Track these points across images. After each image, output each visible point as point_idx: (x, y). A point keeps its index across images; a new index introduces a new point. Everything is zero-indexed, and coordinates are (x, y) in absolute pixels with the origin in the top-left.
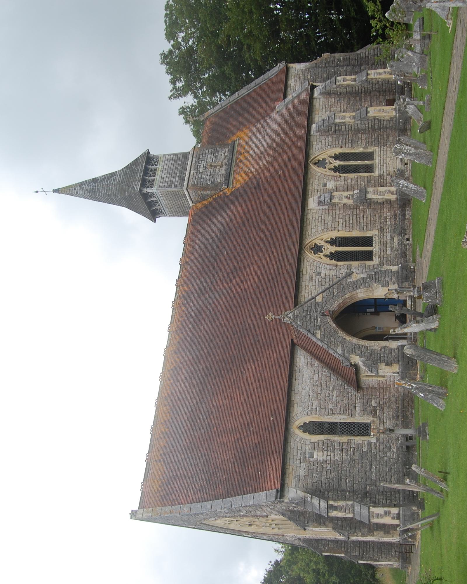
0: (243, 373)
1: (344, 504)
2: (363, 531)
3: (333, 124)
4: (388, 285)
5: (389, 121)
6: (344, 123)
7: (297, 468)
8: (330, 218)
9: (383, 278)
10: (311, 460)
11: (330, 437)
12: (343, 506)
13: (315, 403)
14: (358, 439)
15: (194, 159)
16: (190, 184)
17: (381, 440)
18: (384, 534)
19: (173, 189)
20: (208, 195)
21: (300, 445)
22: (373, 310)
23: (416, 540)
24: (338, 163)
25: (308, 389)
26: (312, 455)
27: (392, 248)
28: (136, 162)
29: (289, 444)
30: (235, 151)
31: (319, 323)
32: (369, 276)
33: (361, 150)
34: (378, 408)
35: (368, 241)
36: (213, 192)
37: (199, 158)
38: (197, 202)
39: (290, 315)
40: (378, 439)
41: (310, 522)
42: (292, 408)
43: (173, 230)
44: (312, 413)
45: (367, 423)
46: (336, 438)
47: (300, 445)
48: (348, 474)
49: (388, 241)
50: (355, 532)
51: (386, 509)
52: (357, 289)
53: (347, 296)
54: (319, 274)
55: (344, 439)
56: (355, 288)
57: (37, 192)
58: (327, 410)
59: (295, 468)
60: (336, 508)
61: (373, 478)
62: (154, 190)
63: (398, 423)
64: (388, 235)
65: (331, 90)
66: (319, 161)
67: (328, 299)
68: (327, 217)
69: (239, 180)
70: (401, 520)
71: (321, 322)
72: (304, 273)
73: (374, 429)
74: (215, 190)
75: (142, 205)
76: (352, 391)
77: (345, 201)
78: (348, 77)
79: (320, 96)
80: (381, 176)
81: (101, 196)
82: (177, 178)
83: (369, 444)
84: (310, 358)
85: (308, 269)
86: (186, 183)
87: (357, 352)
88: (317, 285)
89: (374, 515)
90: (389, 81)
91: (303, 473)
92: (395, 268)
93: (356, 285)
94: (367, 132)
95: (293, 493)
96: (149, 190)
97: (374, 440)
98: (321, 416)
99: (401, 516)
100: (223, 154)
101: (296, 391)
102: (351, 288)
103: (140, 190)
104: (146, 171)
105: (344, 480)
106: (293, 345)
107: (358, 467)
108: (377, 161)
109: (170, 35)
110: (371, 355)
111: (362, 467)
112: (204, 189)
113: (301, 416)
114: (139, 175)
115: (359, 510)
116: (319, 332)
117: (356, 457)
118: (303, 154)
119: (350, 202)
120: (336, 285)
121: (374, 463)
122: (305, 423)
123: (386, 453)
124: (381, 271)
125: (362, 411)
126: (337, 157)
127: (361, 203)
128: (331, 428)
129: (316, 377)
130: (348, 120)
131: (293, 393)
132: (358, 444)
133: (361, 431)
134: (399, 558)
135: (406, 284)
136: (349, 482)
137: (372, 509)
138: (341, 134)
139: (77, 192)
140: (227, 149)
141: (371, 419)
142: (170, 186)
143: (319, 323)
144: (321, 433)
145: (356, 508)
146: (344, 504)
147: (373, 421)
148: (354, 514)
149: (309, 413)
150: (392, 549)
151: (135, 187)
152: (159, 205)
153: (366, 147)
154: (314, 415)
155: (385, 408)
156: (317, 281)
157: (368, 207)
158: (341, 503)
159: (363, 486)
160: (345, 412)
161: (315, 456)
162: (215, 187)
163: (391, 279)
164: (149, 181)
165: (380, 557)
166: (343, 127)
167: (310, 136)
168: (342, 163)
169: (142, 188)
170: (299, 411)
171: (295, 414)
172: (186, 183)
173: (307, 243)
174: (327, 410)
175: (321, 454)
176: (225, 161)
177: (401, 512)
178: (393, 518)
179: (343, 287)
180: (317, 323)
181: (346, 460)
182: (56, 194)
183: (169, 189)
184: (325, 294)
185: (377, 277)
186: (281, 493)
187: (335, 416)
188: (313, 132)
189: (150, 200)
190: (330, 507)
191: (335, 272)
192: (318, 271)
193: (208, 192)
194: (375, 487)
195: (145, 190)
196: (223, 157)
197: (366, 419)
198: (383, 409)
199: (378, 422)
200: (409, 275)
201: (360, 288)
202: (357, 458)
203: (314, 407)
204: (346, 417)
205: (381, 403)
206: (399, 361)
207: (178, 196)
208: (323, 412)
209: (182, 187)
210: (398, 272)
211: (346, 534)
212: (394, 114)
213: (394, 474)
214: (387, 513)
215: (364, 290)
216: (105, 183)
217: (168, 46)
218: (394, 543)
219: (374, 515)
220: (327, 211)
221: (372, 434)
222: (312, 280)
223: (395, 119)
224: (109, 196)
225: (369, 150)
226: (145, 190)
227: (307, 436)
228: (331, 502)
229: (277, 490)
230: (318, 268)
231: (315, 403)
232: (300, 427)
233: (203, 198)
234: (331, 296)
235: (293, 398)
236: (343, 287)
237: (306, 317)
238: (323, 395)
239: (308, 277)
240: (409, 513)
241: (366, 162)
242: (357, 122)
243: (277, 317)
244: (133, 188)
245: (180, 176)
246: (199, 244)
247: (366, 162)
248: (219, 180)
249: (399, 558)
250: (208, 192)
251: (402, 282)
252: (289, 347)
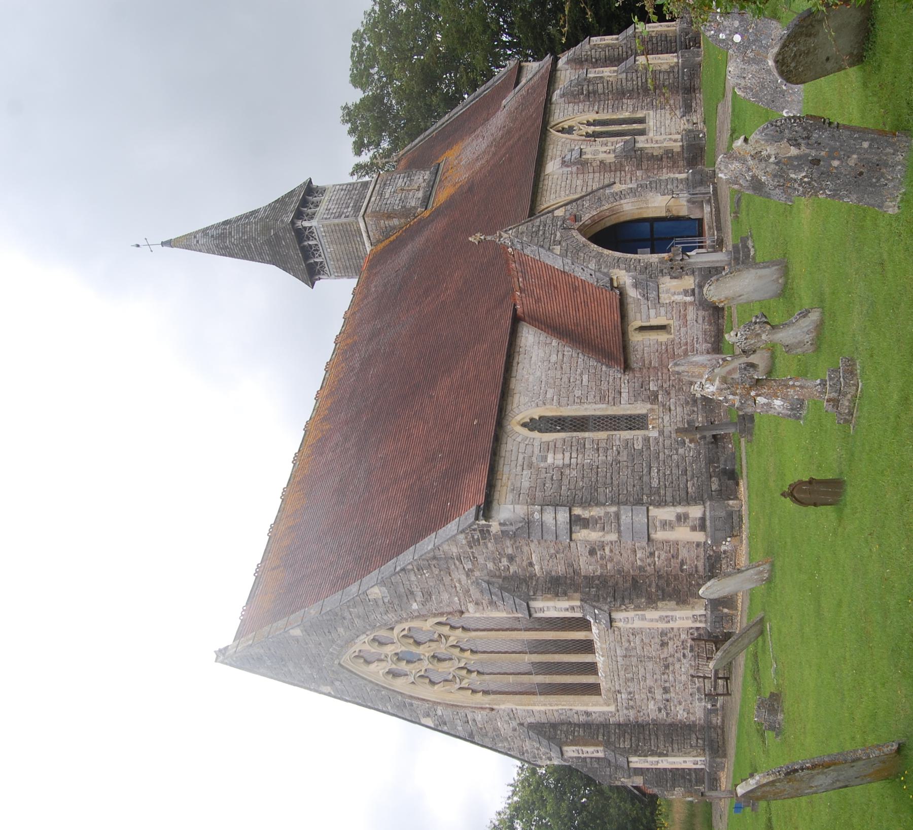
0: (431, 397)
1: (602, 514)
2: (637, 601)
3: (585, 79)
5: (669, 73)
6: (601, 77)
7: (515, 475)
8: (579, 182)
10: (542, 465)
11: (575, 434)
12: (600, 518)
14: (626, 434)
15: (378, 186)
16: (369, 210)
17: (666, 433)
18: (677, 604)
19: (343, 220)
20: (393, 228)
21: (522, 446)
23: (736, 609)
24: (591, 129)
25: (538, 374)
26: (545, 459)
28: (291, 194)
29: (503, 446)
30: (440, 172)
33: (626, 115)
34: (660, 392)
36: (402, 221)
37: (385, 184)
38: (379, 241)
40: (661, 432)
41: (539, 593)
42: (510, 398)
43: (337, 293)
45: (642, 415)
46: (586, 434)
47: (522, 446)
48: (609, 481)
50: (623, 603)
51: (680, 510)
52: (621, 199)
55: (602, 435)
57: (138, 246)
58: (571, 399)
59: (512, 477)
60: (585, 523)
61: (655, 484)
62: (314, 223)
63: (696, 409)
65: (584, 53)
66: (563, 129)
68: (574, 182)
69: (442, 196)
70: (708, 529)
71: (561, 236)
74: (407, 217)
75: (295, 253)
76: (614, 373)
77: (602, 156)
79: (566, 66)
81: (233, 244)
82: (350, 209)
83: (647, 440)
84: (543, 337)
86: (364, 235)
89: (658, 524)
90: (666, 37)
91: (526, 484)
94: (636, 95)
95: (507, 510)
96: (306, 224)
97: (653, 434)
99: (708, 523)
100: (421, 178)
103: (293, 223)
104: (304, 203)
105: (601, 490)
106: (516, 320)
107: (625, 472)
108: (651, 124)
109: (359, 79)
111: (633, 471)
112: (389, 216)
113: (524, 407)
114: (293, 206)
115: (629, 520)
117: (624, 457)
118: (540, 120)
119: (610, 158)
121: (654, 465)
122: (532, 419)
123: (677, 450)
125: (633, 398)
126: (589, 124)
127: (626, 157)
128: (579, 424)
129: (554, 358)
131: (513, 380)
132: (627, 440)
134: (704, 750)
136: (610, 492)
137: (654, 511)
138: (598, 99)
139: (198, 242)
140: (428, 172)
141: (649, 406)
142: (340, 216)
144: (563, 430)
145: (623, 517)
146: (602, 514)
147: (652, 410)
148: (619, 532)
150: (690, 734)
151: (283, 236)
152: (320, 256)
153: (633, 111)
154: (548, 406)
155: (673, 393)
157: (638, 165)
158: (596, 512)
159: (636, 496)
160: (602, 399)
161: (550, 460)
162: (406, 212)
164: (308, 215)
165: (670, 749)
166: (600, 86)
167: (551, 104)
169: (295, 220)
171: (515, 405)
172: (364, 235)
173: (543, 207)
174: (571, 399)
175: (559, 456)
176: (423, 185)
177: (708, 514)
178: (694, 529)
181: (605, 463)
182: (166, 249)
183: (337, 221)
184: (569, 207)
186: (486, 509)
187: (586, 406)
188: (554, 99)
189: (306, 243)
190: (575, 522)
193: (396, 222)
194: (657, 498)
195: (299, 224)
196: (421, 180)
197: (640, 408)
198: (669, 394)
202: (625, 459)
203: (549, 395)
204: (604, 406)
205: (665, 386)
207: (348, 234)
208: (564, 401)
209: (356, 217)
211: (606, 608)
212: (675, 60)
213: (692, 478)
214: (682, 519)
216: (242, 222)
217: (356, 96)
218: (695, 725)
219: (658, 524)
220: (574, 176)
221: (650, 427)
223: (676, 70)
224: (245, 241)
225: (640, 115)
226: (299, 224)
227: (536, 434)
228: (577, 511)
229: (478, 507)
232: (524, 425)
233: (386, 233)
235: (512, 386)
237: (537, 232)
238: (565, 379)
240: (723, 514)
242: (620, 77)
243: (489, 238)
244: (282, 221)
245: (354, 206)
246: (375, 286)
248: (413, 204)
249: (704, 750)
250: (396, 222)
252: (509, 322)
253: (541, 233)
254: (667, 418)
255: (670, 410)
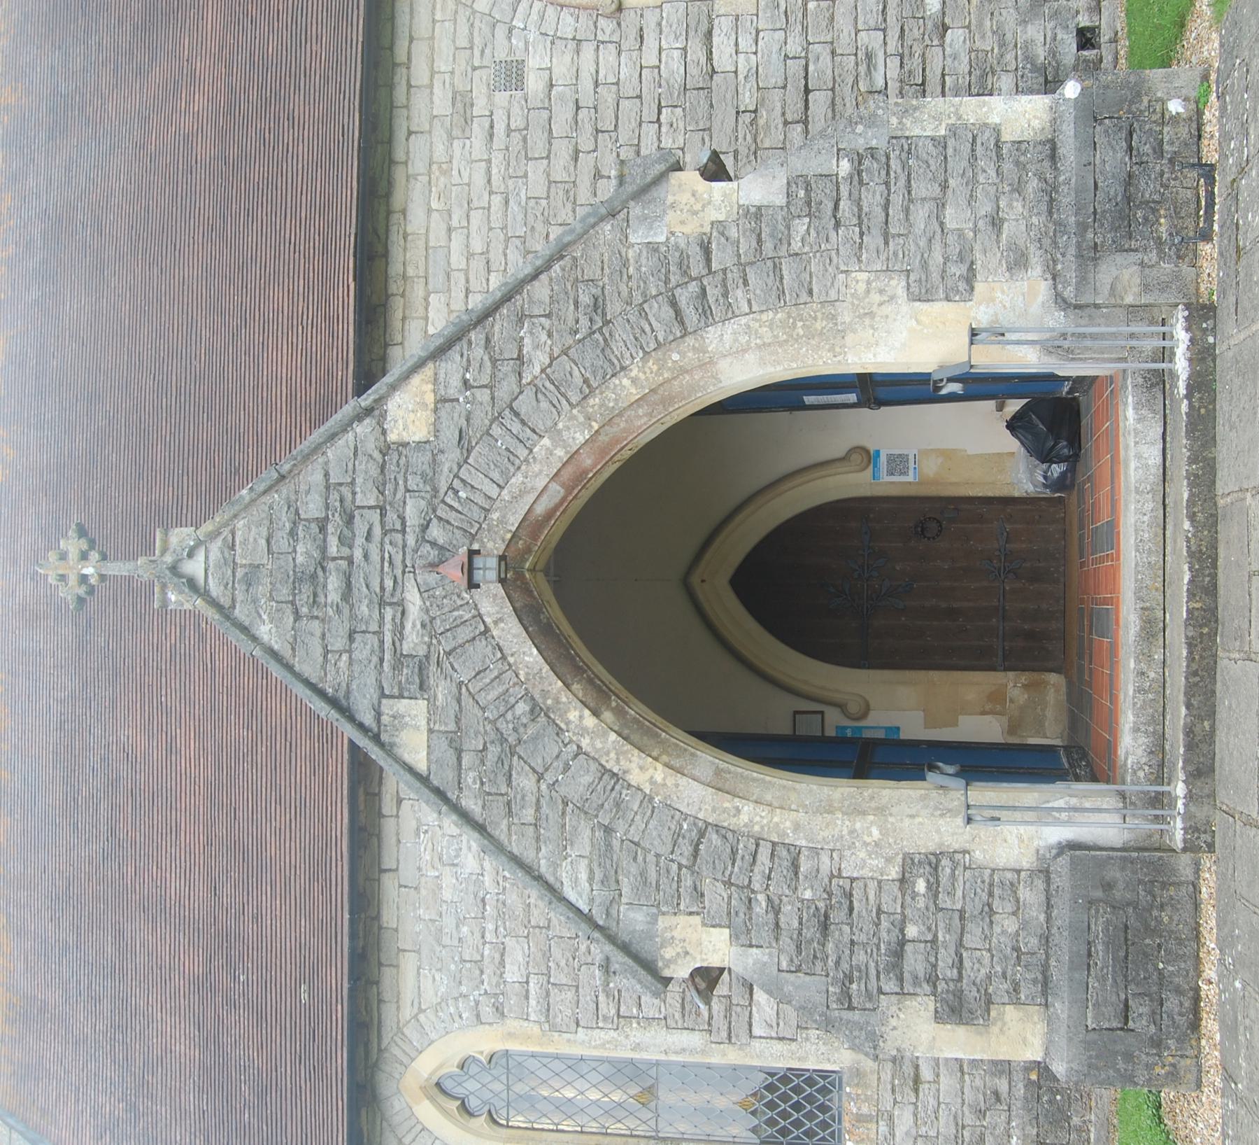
4: (970, 278)
9: (920, 214)
13: (516, 953)
22: (852, 398)
31: (413, 640)
32: (807, 196)
39: (195, 567)
42: (387, 972)
44: (499, 1011)
45: (824, 1074)
53: (626, 388)
54: (513, 75)
56: (691, 316)
67: (481, 419)
72: (420, 73)
73: (860, 1119)
85: (444, 46)
87: (715, 894)
88: (497, 158)
92: (1020, 114)
93: (696, 286)
98: (553, 1028)
101: (407, 873)
102: (660, 312)
110: (825, 926)
116: (415, 710)
120: (541, 290)
124: (908, 147)
131: (389, 884)
133: (784, 1115)
135: (1122, 275)
143: (413, 640)
147: (858, 1073)
149: (487, 1010)
154: (513, 1024)
156: (500, 128)
163: (996, 223)
170: (429, 997)
171: (407, 1012)
179: (597, 305)
180: (399, 631)
184: (451, 368)
185: (872, 198)
187: (636, 1034)
191: (608, 56)
192: (501, 55)
199: (887, 1076)
200: (1147, 189)
201: (730, 313)
203: (513, 974)
204: (695, 1040)
206: (1045, 983)
208: (562, 1001)
210: (1052, 149)
215: (766, 325)
222: (467, 121)
230: (501, 31)
231: (516, 953)
234: (503, 393)
235: (389, 917)
236: (597, 305)
237: (313, 578)
239: (441, 103)
243: (116, 569)
251: (1090, 256)
253: (334, 583)
254: (904, 1120)
255: (917, 1080)
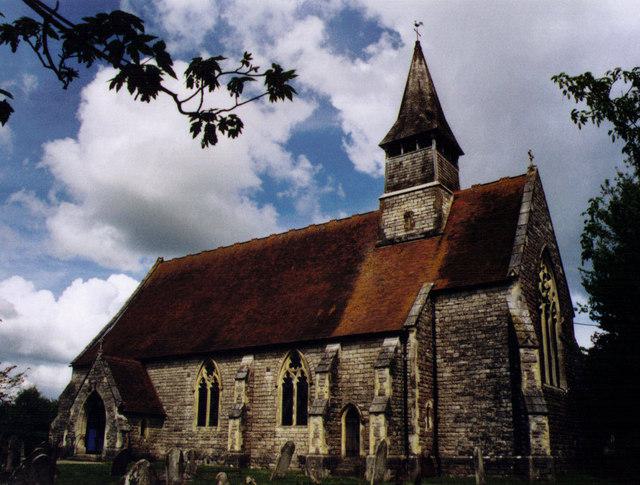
27: (203, 446)
35: (214, 422)
49: (210, 442)
64: (215, 442)
78: (387, 385)
80: (274, 434)
130: (318, 390)
168: (295, 387)
241: (294, 417)
247: (294, 417)
